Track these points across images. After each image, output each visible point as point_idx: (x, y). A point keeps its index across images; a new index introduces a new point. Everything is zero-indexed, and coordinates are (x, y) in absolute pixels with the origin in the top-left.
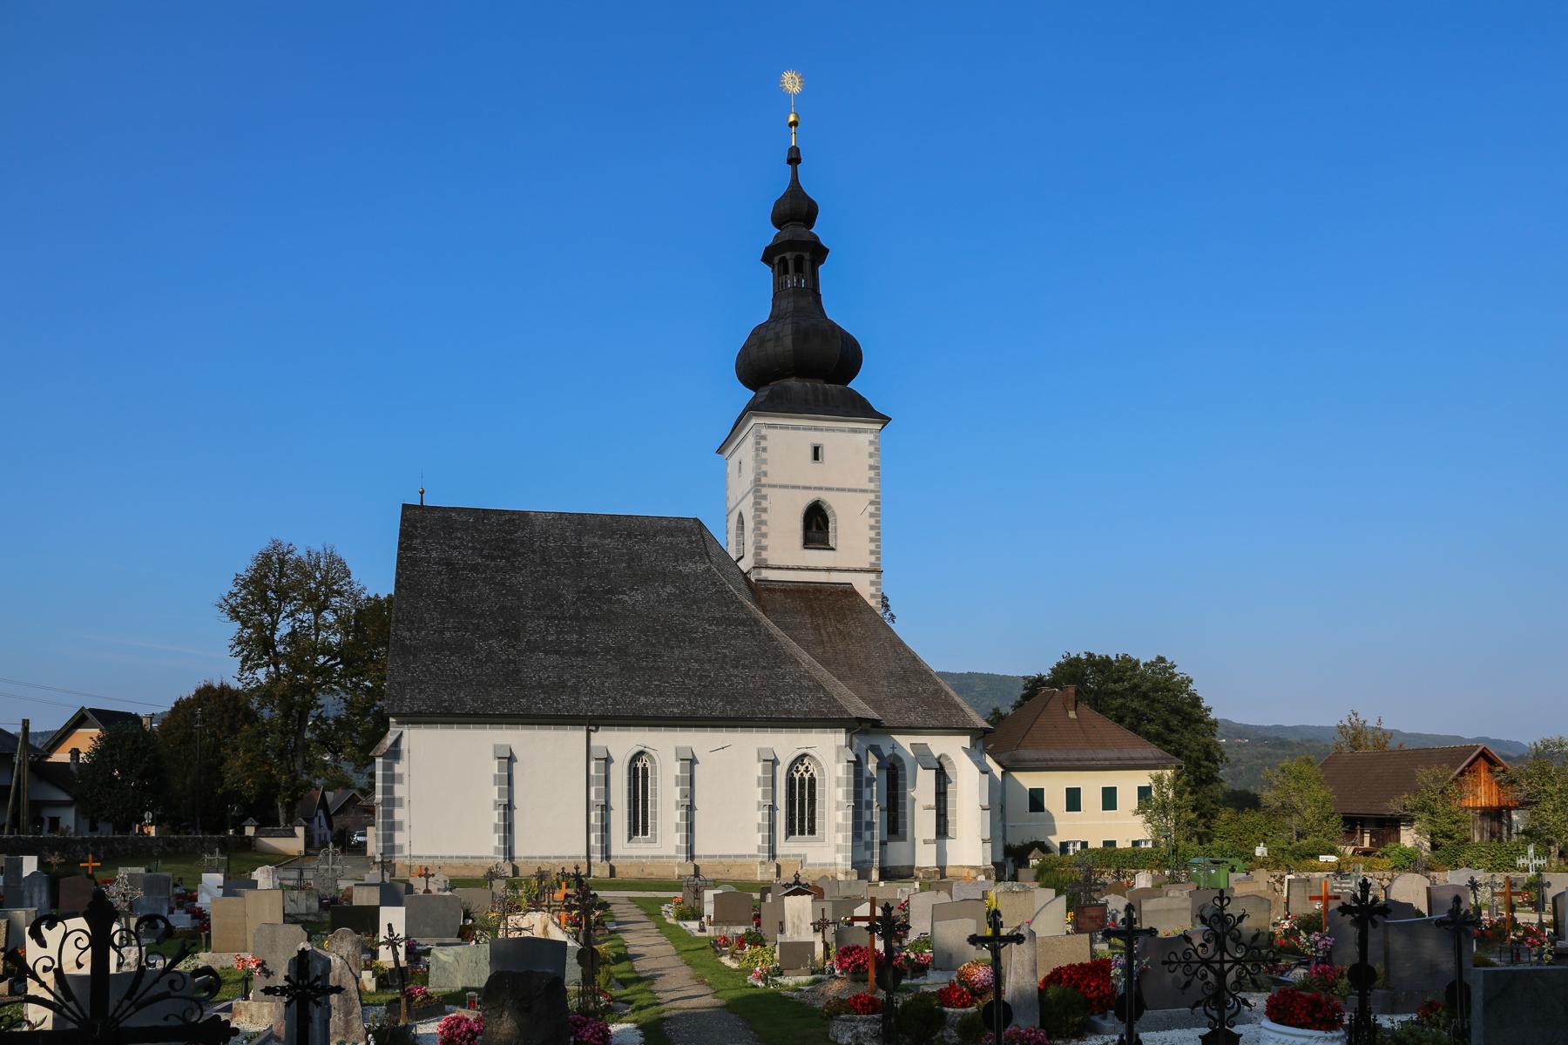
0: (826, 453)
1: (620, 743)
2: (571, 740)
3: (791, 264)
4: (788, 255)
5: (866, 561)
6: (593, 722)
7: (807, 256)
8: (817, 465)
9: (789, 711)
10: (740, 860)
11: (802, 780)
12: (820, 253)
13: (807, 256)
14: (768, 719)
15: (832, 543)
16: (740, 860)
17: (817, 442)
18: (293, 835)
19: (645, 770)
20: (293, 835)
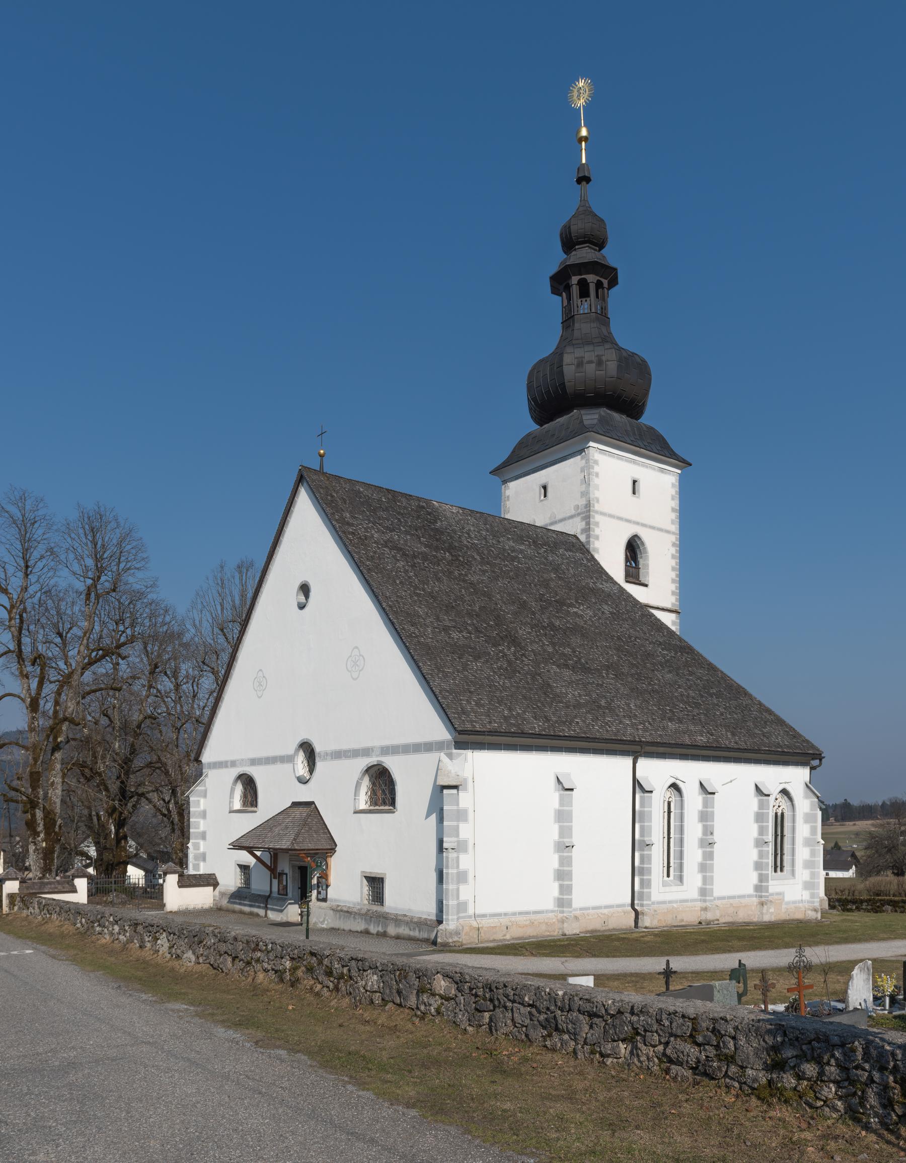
0: (642, 487)
1: (657, 771)
2: (614, 770)
3: (592, 288)
4: (591, 278)
5: (669, 601)
6: (636, 749)
7: (605, 283)
8: (633, 499)
9: (779, 745)
10: (743, 901)
11: (776, 814)
12: (613, 282)
13: (605, 283)
14: (770, 752)
15: (642, 579)
16: (743, 901)
17: (636, 477)
18: (74, 890)
19: (669, 803)
20: (74, 890)
